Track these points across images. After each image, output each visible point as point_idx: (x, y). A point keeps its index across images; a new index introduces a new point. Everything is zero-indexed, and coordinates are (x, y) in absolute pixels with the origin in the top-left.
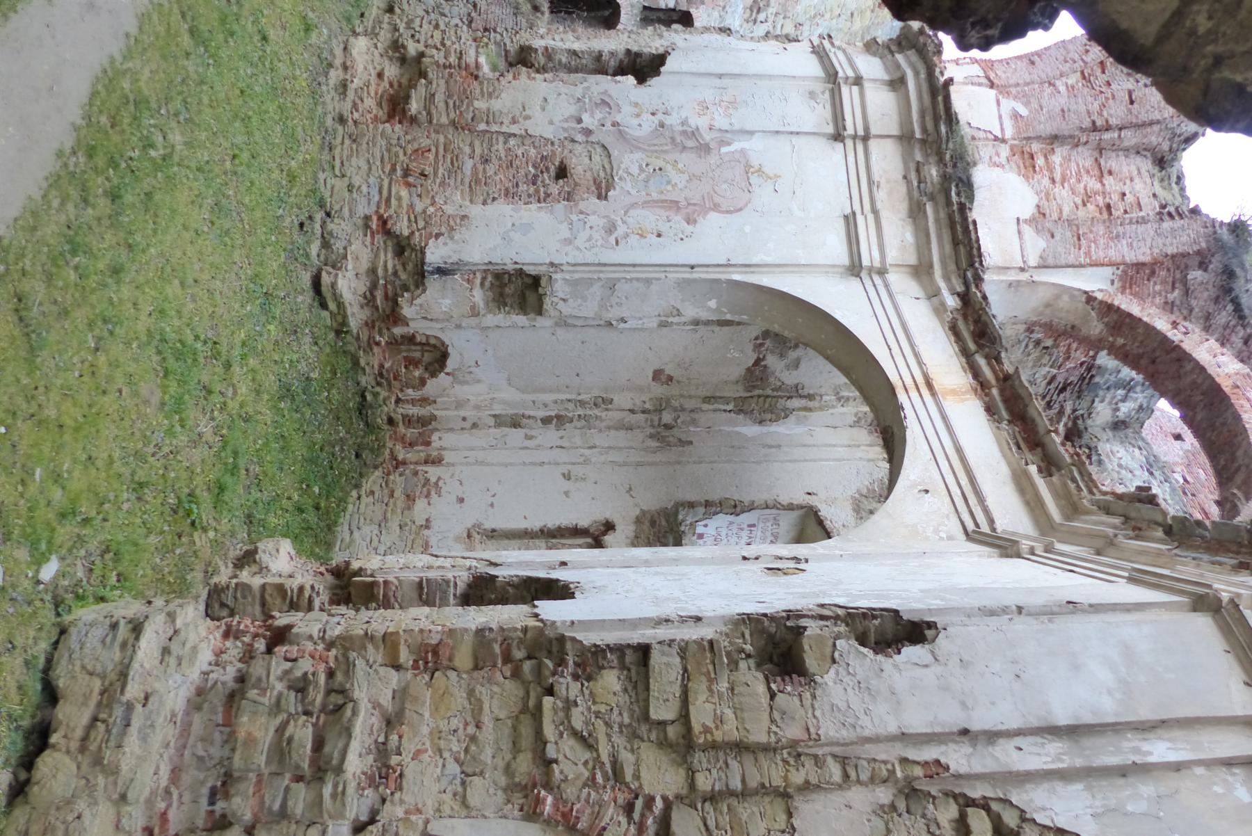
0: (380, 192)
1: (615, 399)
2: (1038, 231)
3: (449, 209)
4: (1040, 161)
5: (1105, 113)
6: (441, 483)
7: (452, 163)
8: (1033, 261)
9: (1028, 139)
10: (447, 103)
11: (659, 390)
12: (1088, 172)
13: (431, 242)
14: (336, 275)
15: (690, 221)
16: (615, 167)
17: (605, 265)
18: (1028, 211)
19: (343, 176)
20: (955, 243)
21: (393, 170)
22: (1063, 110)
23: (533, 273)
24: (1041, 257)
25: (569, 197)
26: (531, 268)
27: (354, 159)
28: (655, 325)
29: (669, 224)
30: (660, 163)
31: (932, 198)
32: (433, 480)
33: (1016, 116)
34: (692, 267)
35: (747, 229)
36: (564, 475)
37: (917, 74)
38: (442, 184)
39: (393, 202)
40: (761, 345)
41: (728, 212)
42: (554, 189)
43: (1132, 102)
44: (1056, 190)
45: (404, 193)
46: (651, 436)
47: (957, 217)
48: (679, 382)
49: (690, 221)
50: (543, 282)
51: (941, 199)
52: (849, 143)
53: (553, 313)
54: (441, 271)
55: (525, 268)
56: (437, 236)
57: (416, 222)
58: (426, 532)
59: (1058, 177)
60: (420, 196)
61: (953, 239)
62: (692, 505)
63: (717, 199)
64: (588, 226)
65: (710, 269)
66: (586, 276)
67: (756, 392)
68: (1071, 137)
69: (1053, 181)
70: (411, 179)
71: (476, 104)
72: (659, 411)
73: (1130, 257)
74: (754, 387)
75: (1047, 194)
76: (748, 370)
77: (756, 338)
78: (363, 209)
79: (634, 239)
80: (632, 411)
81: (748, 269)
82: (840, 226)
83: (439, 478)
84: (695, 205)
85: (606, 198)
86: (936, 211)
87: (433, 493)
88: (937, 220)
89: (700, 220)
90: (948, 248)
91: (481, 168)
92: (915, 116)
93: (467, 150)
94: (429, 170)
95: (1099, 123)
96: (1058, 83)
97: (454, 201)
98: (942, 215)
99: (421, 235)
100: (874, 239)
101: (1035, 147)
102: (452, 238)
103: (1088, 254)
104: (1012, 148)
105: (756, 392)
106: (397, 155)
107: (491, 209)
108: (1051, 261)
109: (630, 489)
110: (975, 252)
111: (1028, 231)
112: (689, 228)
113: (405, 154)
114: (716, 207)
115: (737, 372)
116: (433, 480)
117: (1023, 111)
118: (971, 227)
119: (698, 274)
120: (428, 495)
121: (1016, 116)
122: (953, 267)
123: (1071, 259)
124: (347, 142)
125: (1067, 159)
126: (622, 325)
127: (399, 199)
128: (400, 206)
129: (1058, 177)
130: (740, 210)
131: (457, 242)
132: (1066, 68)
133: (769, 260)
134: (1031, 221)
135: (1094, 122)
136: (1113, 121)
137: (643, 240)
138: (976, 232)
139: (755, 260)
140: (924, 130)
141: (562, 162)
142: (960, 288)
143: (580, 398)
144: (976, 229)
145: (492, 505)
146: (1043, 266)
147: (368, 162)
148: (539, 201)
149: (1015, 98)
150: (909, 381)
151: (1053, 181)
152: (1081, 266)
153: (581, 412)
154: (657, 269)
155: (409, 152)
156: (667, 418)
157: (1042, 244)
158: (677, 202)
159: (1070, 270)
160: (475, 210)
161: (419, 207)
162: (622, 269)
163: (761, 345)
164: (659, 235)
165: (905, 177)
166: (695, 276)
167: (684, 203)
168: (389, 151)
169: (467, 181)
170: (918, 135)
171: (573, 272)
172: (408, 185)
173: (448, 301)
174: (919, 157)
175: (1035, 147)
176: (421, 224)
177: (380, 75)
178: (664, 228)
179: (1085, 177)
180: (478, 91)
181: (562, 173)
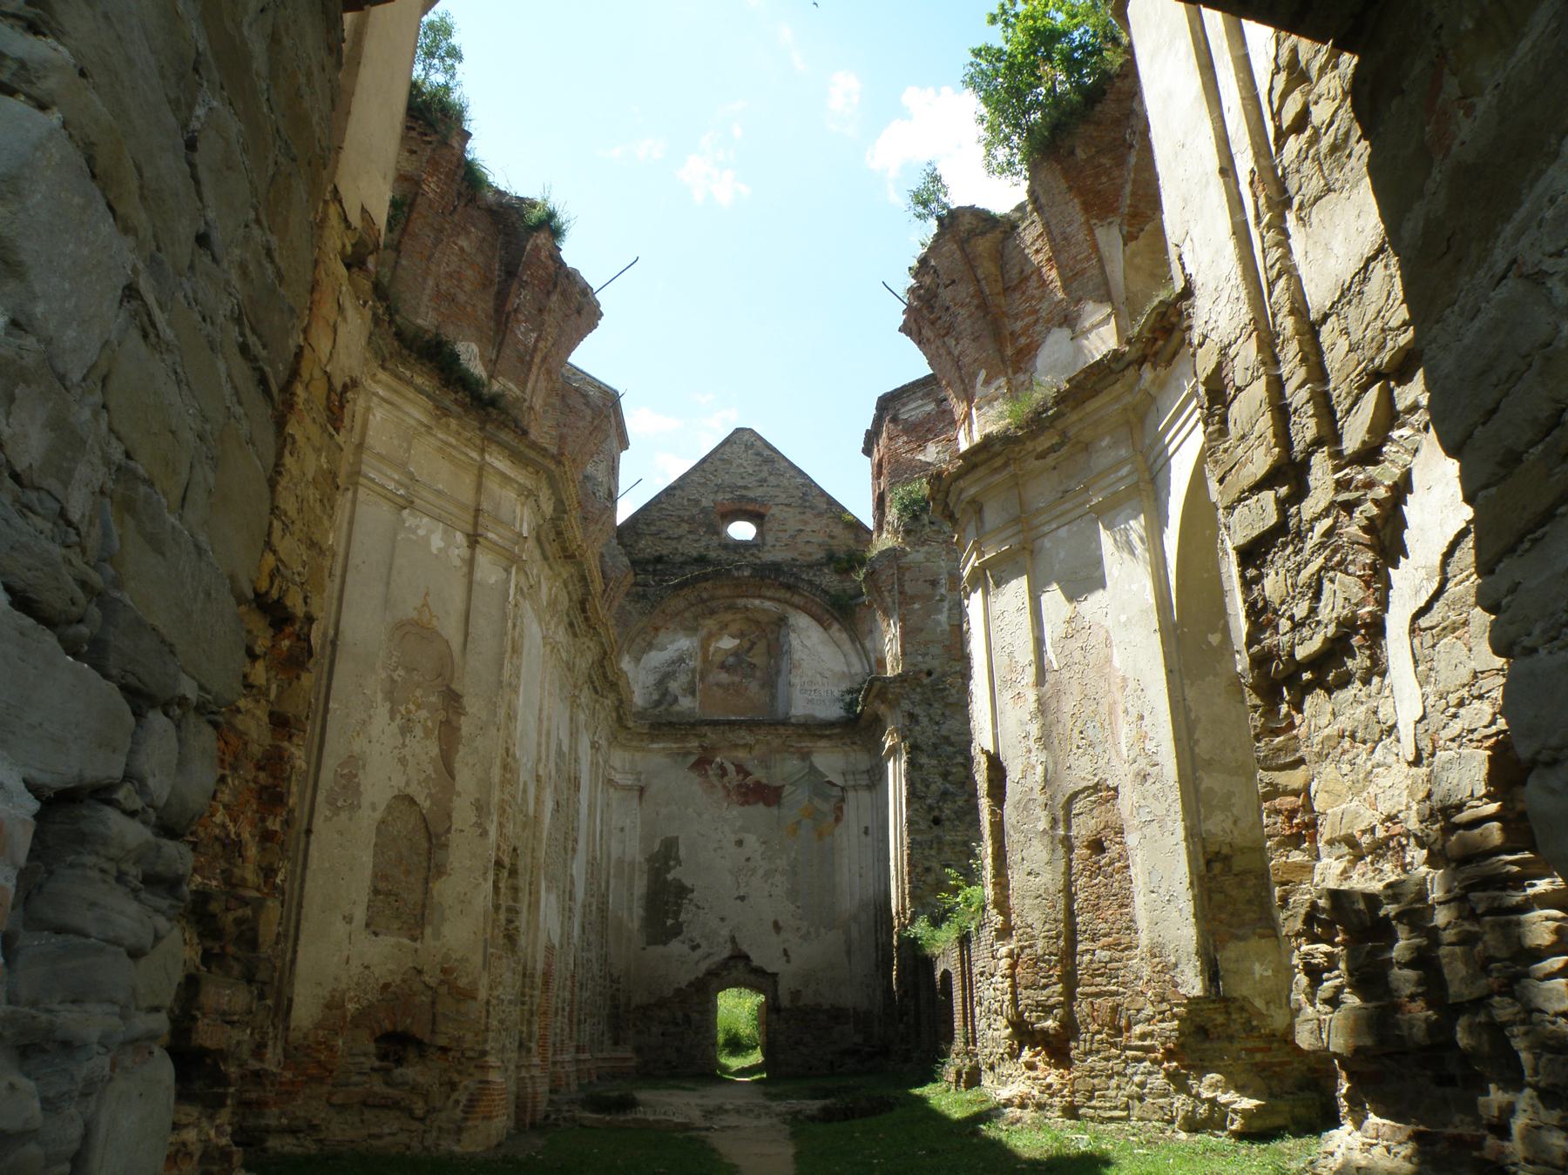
0: (1139, 1060)
3: (1146, 973)
4: (1023, 341)
7: (1102, 975)
9: (1003, 361)
10: (1045, 986)
13: (1182, 991)
14: (1235, 1111)
16: (1085, 784)
18: (1066, 333)
19: (1127, 1108)
21: (1115, 1045)
25: (1120, 832)
27: (1112, 1093)
30: (1076, 731)
33: (987, 382)
37: (961, 491)
38: (1124, 984)
39: (1148, 1042)
42: (1113, 851)
45: (1138, 1029)
51: (1060, 425)
54: (1212, 972)
56: (1176, 985)
57: (1163, 1012)
59: (1032, 319)
60: (1139, 1011)
64: (1143, 803)
69: (1036, 322)
70: (1123, 1023)
71: (1040, 952)
73: (1080, 218)
75: (1048, 321)
78: (1159, 1081)
85: (1116, 789)
91: (1104, 940)
93: (1087, 958)
94: (1110, 1002)
95: (975, 302)
96: (956, 353)
97: (1139, 965)
99: (1178, 1005)
101: (1009, 351)
102: (1176, 965)
103: (1088, 259)
104: (1015, 373)
106: (1102, 1042)
107: (1142, 923)
108: (1102, 292)
113: (1099, 1032)
117: (982, 375)
121: (987, 382)
123: (1096, 272)
124: (1094, 1103)
125: (1016, 317)
127: (1143, 1036)
128: (1151, 1035)
129: (1032, 319)
131: (1178, 958)
132: (942, 351)
135: (977, 307)
136: (972, 290)
137: (1150, 735)
141: (1087, 847)
142: (1132, 371)
147: (1110, 1077)
148: (1127, 867)
149: (973, 387)
151: (1036, 322)
152: (1100, 260)
155: (1096, 1027)
159: (1108, 269)
160: (1144, 939)
161: (1149, 1010)
164: (1142, 718)
168: (1098, 1052)
169: (1117, 955)
172: (1129, 1028)
173: (1257, 968)
175: (1009, 351)
176: (1165, 1006)
177: (1031, 1066)
179: (1030, 292)
180: (1028, 951)
181: (1097, 846)
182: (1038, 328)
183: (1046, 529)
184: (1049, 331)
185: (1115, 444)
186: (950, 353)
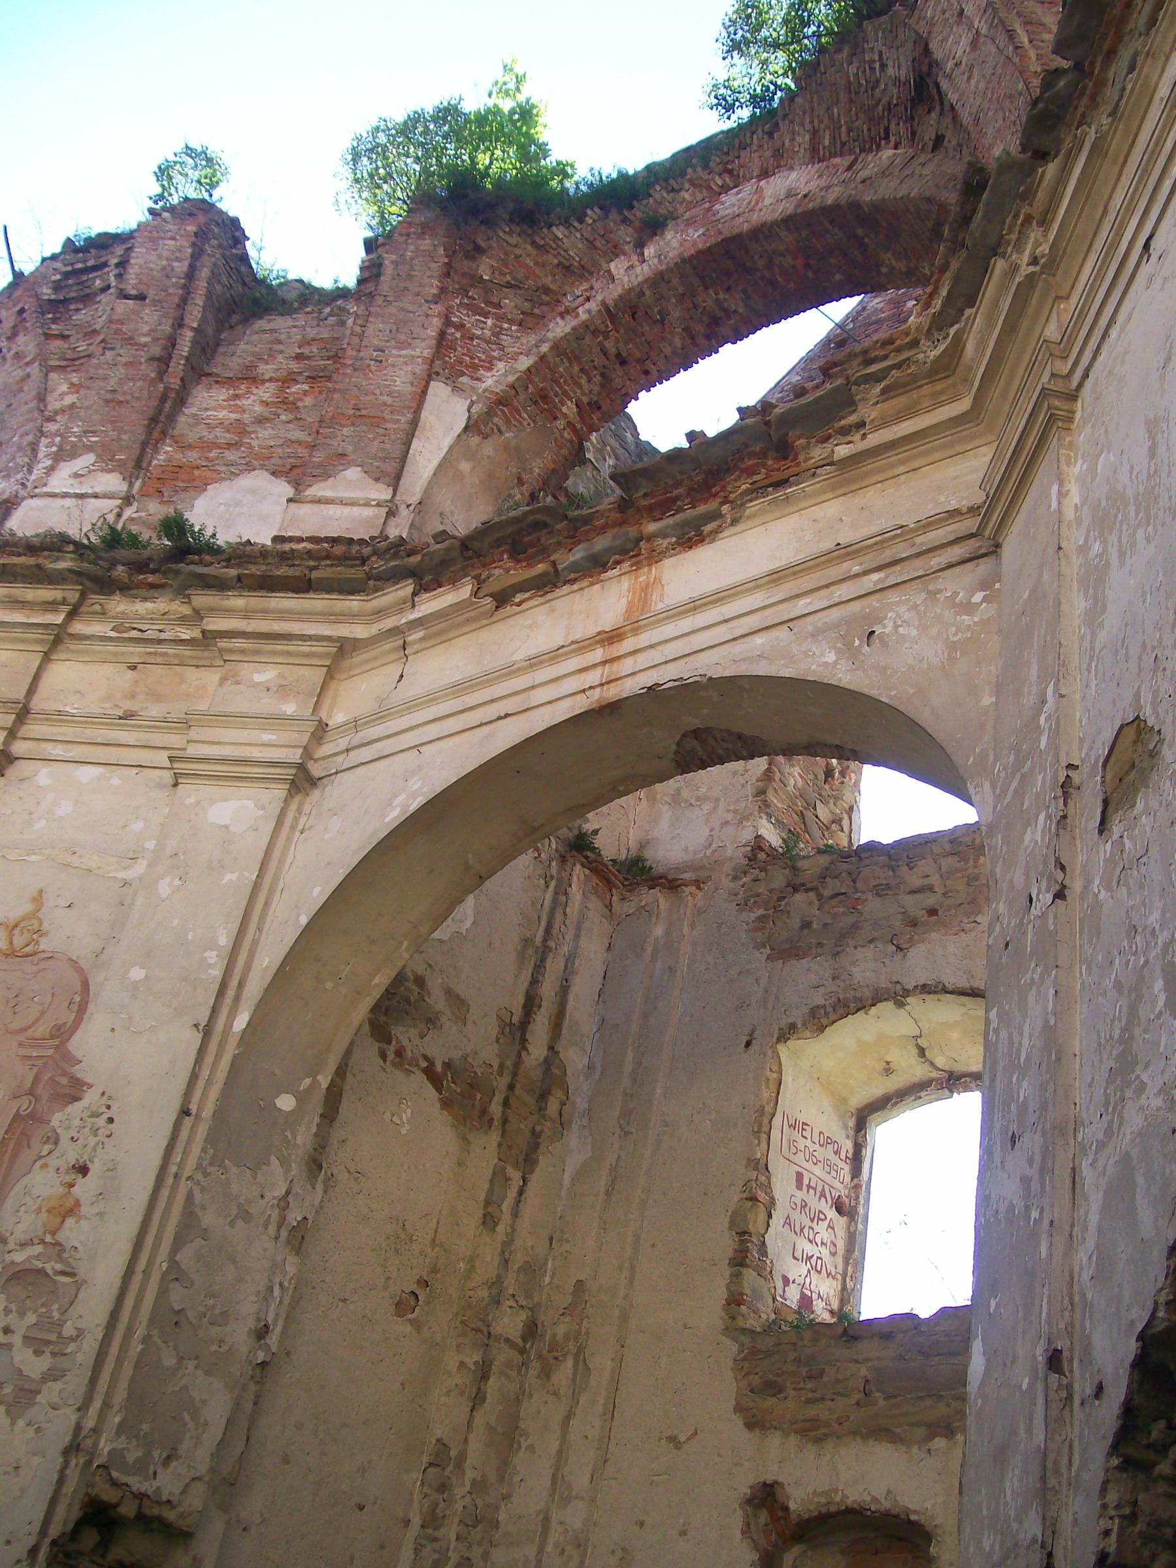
1: (438, 1432)
2: (326, 476)
5: (144, 340)
8: (384, 493)
12: (237, 397)
15: (74, 1090)
17: (114, 1316)
18: (284, 489)
20: (303, 586)
22: (107, 402)
23: (76, 1514)
24: (377, 480)
26: (60, 1512)
28: (296, 1260)
29: (64, 1141)
31: (198, 615)
34: (185, 1112)
35: (137, 974)
40: (399, 1053)
41: (83, 1008)
43: (141, 297)
44: (255, 443)
46: (546, 1374)
47: (255, 570)
48: (434, 1270)
49: (74, 1090)
50: (109, 1495)
51: (203, 599)
52: (18, 748)
53: (196, 1500)
55: (54, 1531)
61: (297, 591)
62: (735, 1300)
63: (41, 1030)
66: (128, 1369)
67: (496, 1109)
68: (163, 399)
69: (236, 445)
73: (423, 350)
74: (484, 1111)
75: (257, 457)
76: (446, 1104)
77: (383, 1056)
79: (72, 1233)
80: (478, 1399)
81: (230, 993)
82: (190, 793)
84: (37, 1079)
86: (229, 612)
88: (246, 614)
89: (77, 1071)
90: (316, 602)
92: (18, 617)
95: (157, 351)
98: (237, 601)
100: (243, 735)
105: (496, 1109)
108: (391, 467)
109: (672, 1439)
110: (339, 550)
111: (319, 490)
112: (90, 1098)
114: (62, 1034)
115: (441, 1133)
118: (287, 547)
119: (207, 1103)
122: (353, 603)
126: (273, 1339)
130: (85, 985)
132: (31, 389)
133: (224, 940)
134: (297, 485)
137: (84, 1210)
138: (300, 540)
139: (217, 973)
140: (51, 606)
143: (416, 1521)
144: (291, 539)
146: (395, 481)
150: (594, 677)
152: (415, 423)
153: (450, 1531)
154: (165, 1193)
156: (509, 1323)
157: (353, 473)
158: (17, 1117)
159: (416, 444)
162: (137, 1278)
163: (399, 1053)
164: (83, 1170)
165: (133, 668)
166: (207, 1113)
167: (24, 1104)
170: (59, 619)
171: (106, 1405)
174: (97, 628)
178: (70, 1154)
182: (231, 455)
183: (57, 751)
184: (250, 468)
185: (283, 690)
186: (41, 398)
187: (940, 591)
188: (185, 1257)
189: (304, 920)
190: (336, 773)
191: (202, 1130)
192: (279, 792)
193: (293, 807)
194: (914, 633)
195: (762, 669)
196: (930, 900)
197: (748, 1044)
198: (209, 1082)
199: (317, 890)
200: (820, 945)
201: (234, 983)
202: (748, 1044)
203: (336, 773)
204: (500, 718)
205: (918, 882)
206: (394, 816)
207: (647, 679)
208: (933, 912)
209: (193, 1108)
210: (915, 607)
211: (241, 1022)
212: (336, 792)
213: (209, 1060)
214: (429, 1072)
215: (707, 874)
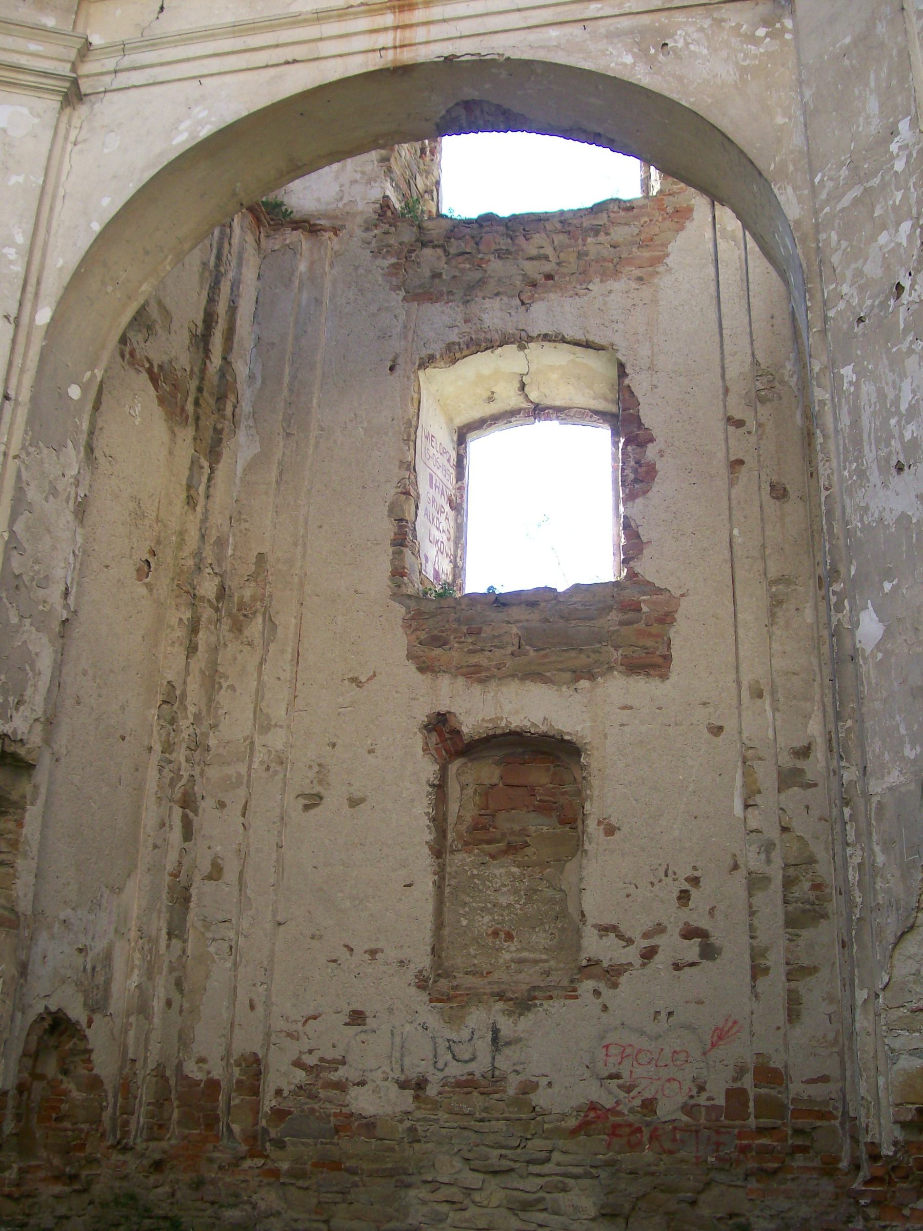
6: (311, 1060)
11: (163, 581)
32: (300, 1076)
36: (307, 807)
46: (238, 628)
58: (432, 1091)
62: (398, 573)
65: (18, 361)
67: (190, 407)
72: (194, 599)
74: (183, 410)
76: (161, 401)
80: (192, 649)
83: (298, 1064)
87: (334, 1077)
109: (353, 680)
116: (300, 1076)
120: (341, 1086)
139: (18, 268)
143: (158, 748)
145: (373, 953)
150: (386, 39)
153: (180, 755)
156: (208, 587)
163: (132, 354)
187: (723, 20)
188: (19, 527)
189: (97, 227)
190: (105, 92)
191: (22, 414)
192: (52, 103)
193: (65, 119)
194: (705, 52)
195: (560, 58)
196: (548, 267)
197: (392, 369)
198: (22, 371)
199: (106, 202)
200: (450, 293)
201: (33, 280)
202: (392, 369)
203: (105, 92)
204: (287, 63)
205: (534, 252)
206: (183, 139)
207: (447, 49)
208: (549, 277)
209: (12, 393)
210: (702, 30)
211: (44, 316)
212: (111, 108)
213: (20, 348)
214: (150, 371)
215: (340, 223)
